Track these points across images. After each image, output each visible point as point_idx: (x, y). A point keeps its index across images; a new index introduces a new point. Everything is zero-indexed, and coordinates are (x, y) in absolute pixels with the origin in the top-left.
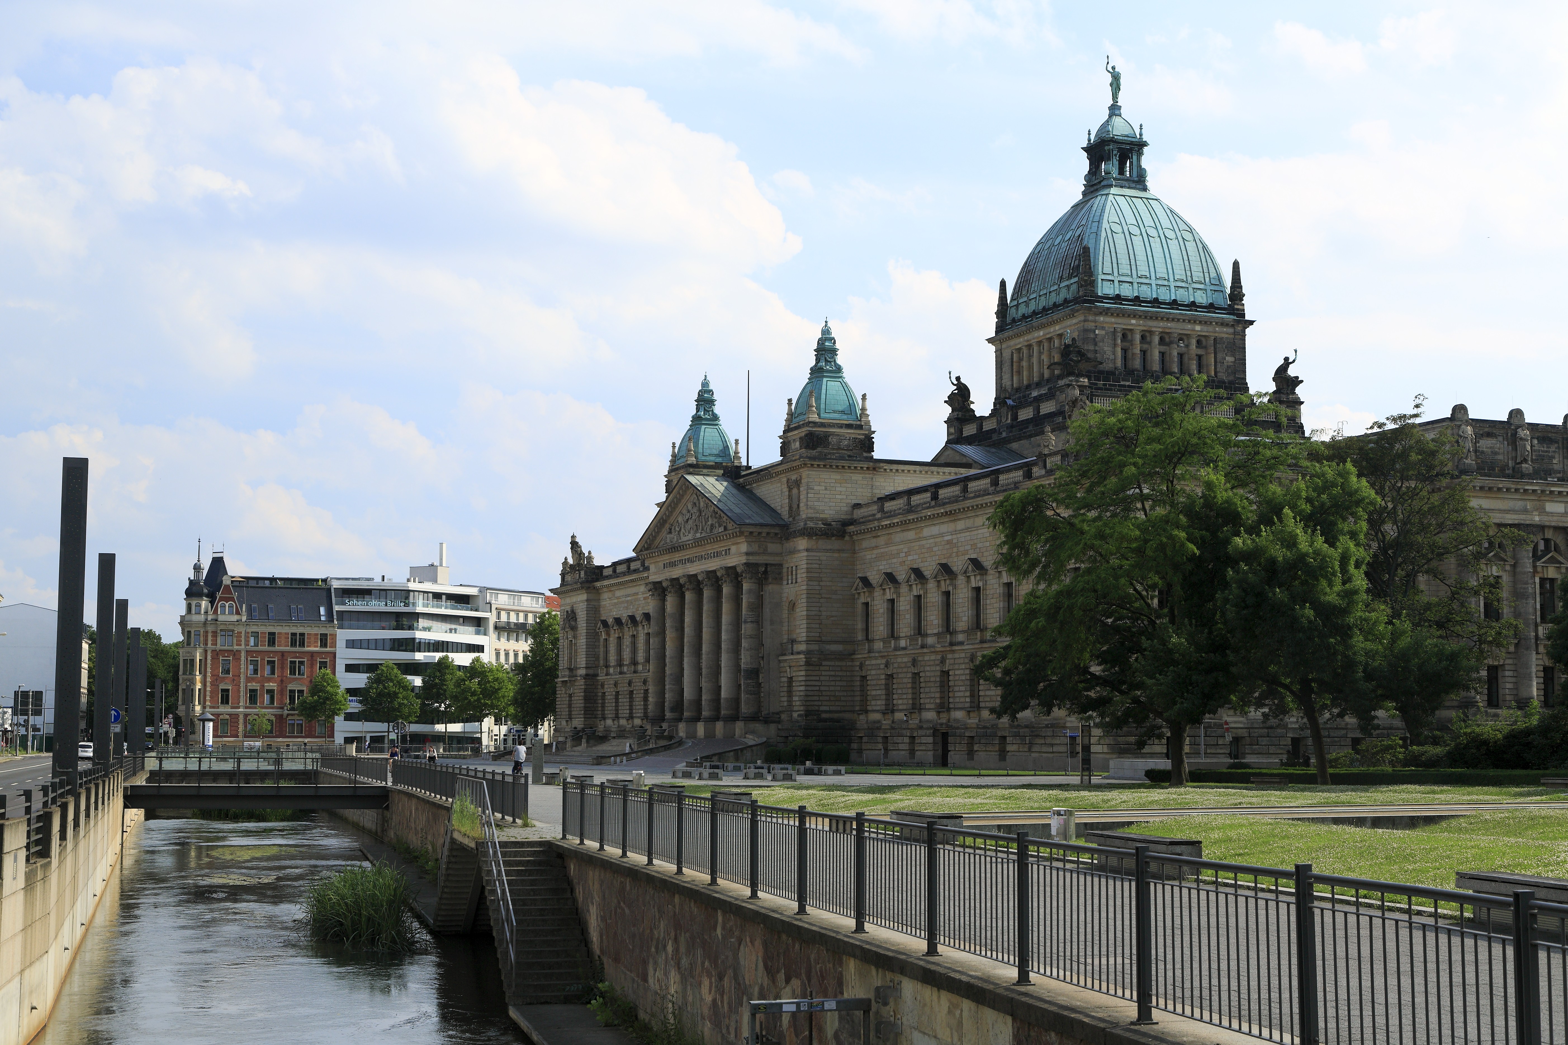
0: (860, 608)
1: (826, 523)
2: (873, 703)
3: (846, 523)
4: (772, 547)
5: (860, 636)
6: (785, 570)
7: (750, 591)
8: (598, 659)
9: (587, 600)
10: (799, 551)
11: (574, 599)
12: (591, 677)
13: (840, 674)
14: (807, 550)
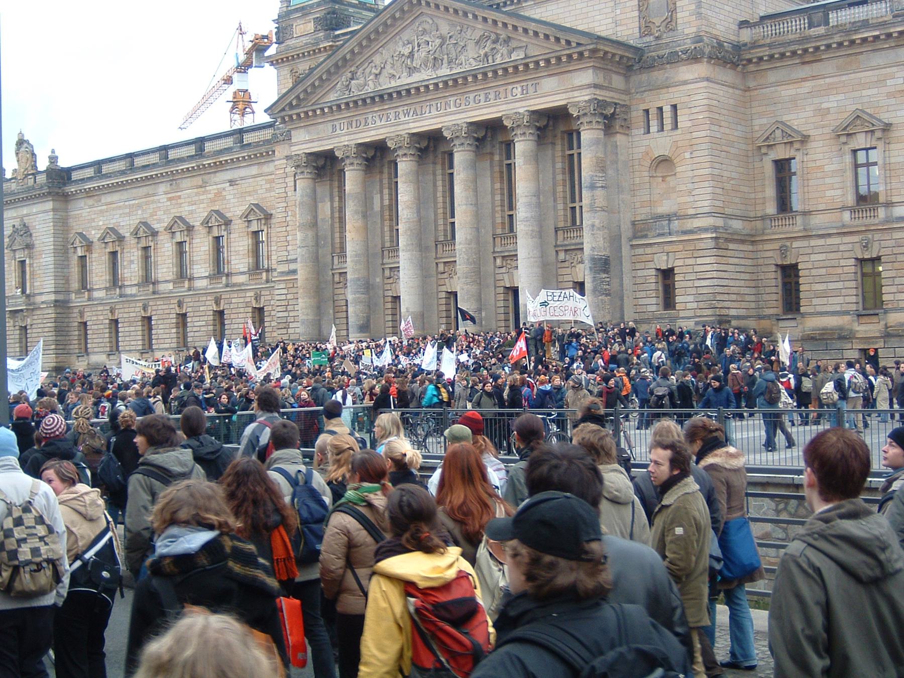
0: (769, 170)
1: (720, 44)
2: (815, 301)
3: (738, 47)
4: (618, 81)
5: (771, 209)
6: (637, 115)
7: (597, 142)
8: (67, 280)
9: (54, 210)
10: (685, 83)
11: (25, 211)
12: (61, 305)
13: (743, 262)
14: (708, 79)
